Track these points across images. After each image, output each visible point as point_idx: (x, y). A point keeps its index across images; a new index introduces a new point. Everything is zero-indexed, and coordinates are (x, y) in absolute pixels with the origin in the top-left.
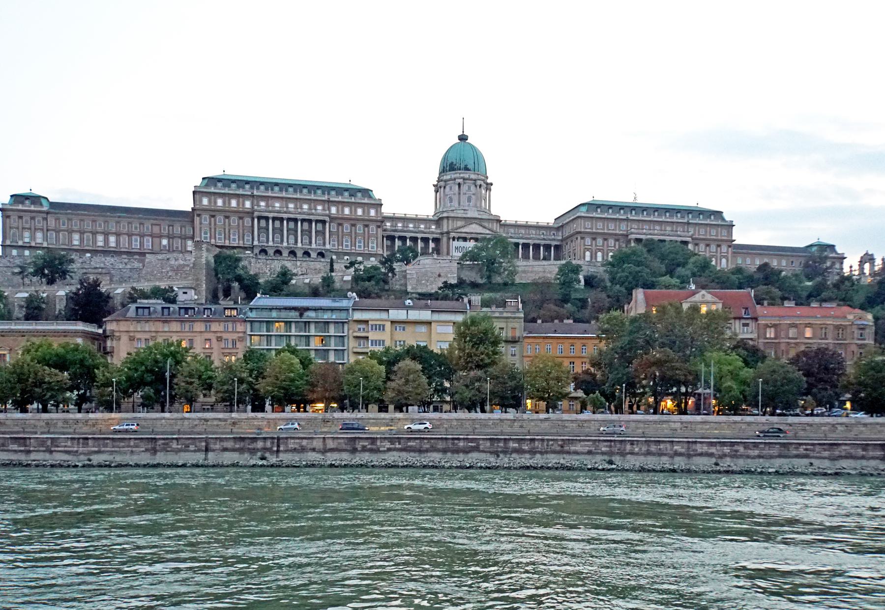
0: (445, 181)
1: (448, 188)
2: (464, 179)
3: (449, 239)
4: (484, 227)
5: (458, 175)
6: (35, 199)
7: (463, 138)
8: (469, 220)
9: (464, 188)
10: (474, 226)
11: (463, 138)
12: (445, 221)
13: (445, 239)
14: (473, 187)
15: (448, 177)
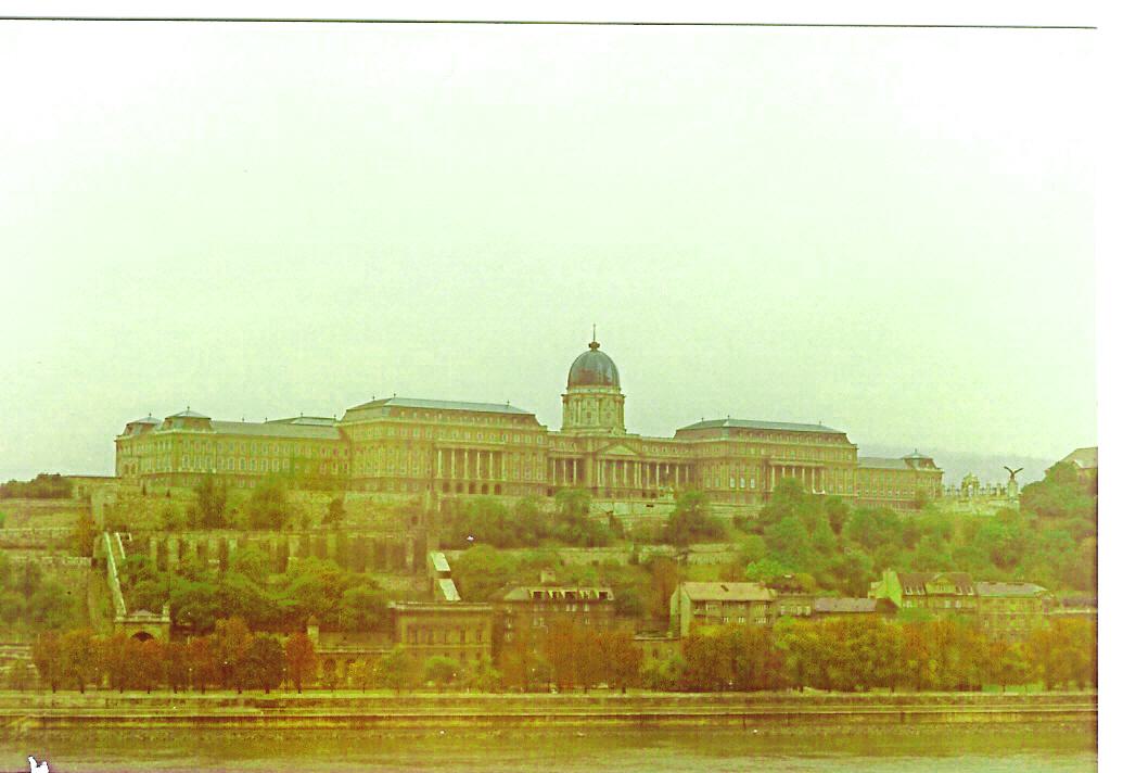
0: (582, 395)
1: (585, 403)
2: (605, 394)
3: (595, 460)
4: (630, 449)
5: (597, 391)
6: (204, 422)
7: (594, 346)
8: (614, 442)
9: (604, 403)
10: (620, 447)
11: (594, 346)
12: (590, 443)
13: (590, 462)
14: (612, 403)
15: (585, 391)
